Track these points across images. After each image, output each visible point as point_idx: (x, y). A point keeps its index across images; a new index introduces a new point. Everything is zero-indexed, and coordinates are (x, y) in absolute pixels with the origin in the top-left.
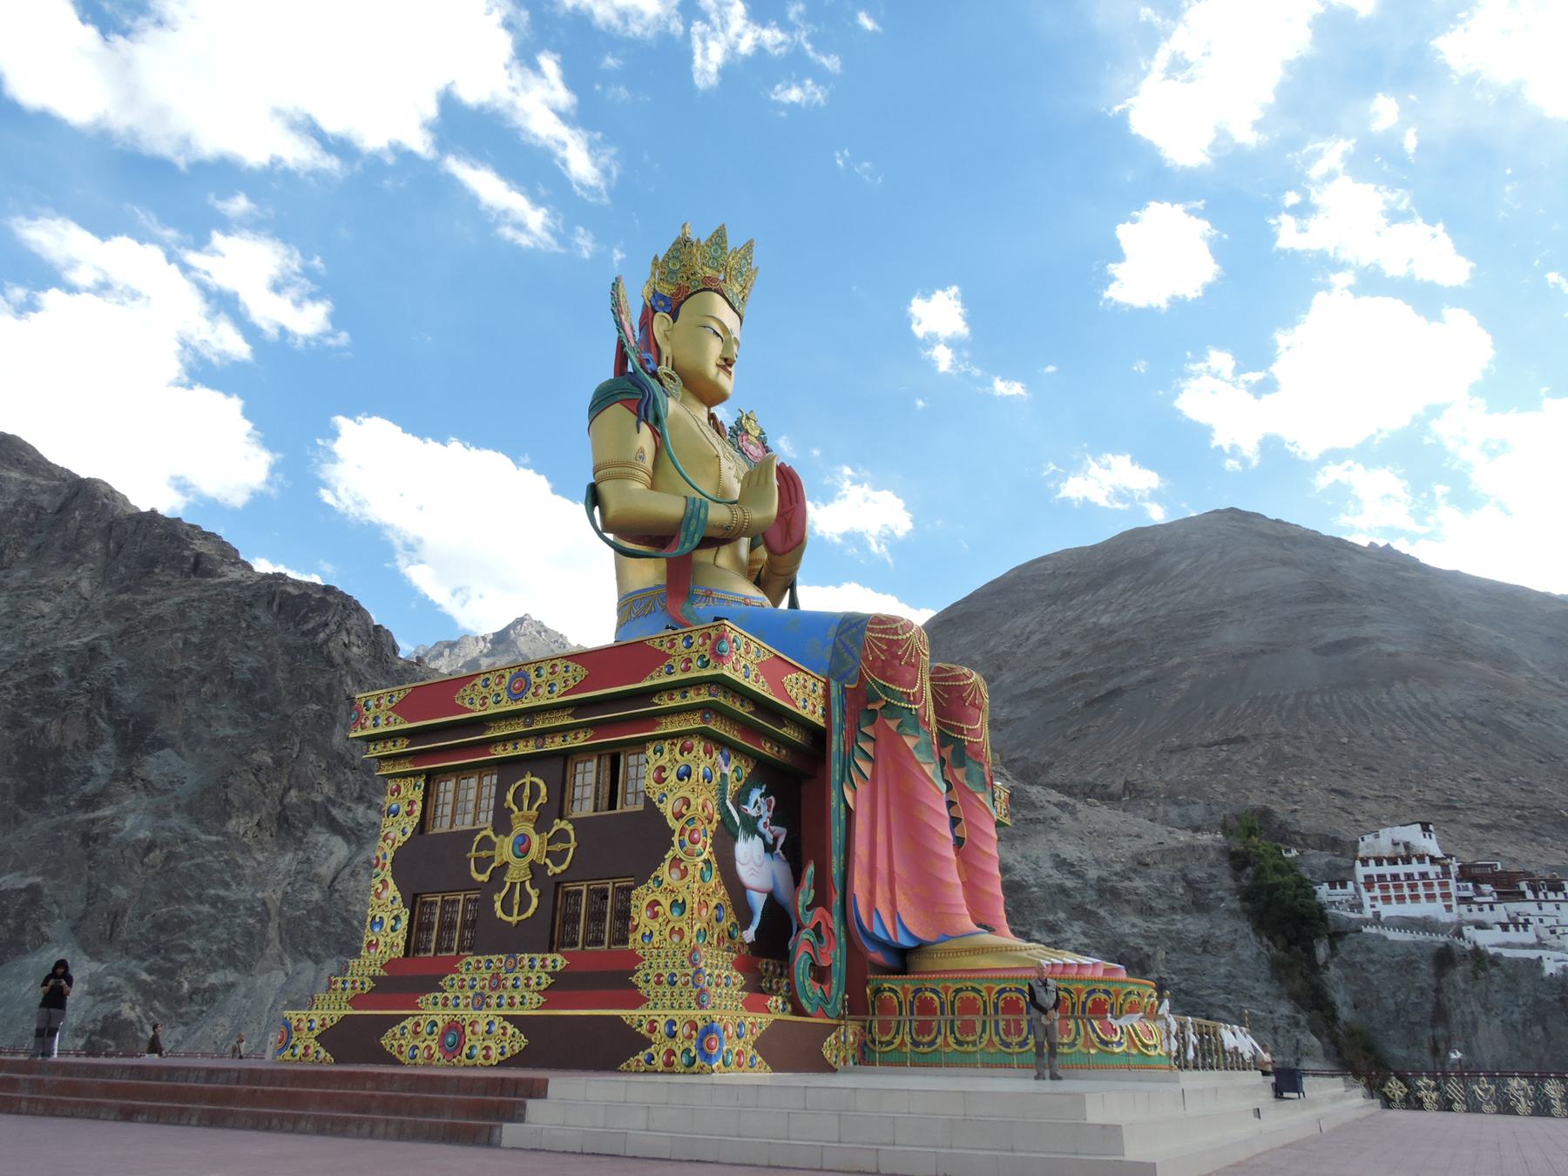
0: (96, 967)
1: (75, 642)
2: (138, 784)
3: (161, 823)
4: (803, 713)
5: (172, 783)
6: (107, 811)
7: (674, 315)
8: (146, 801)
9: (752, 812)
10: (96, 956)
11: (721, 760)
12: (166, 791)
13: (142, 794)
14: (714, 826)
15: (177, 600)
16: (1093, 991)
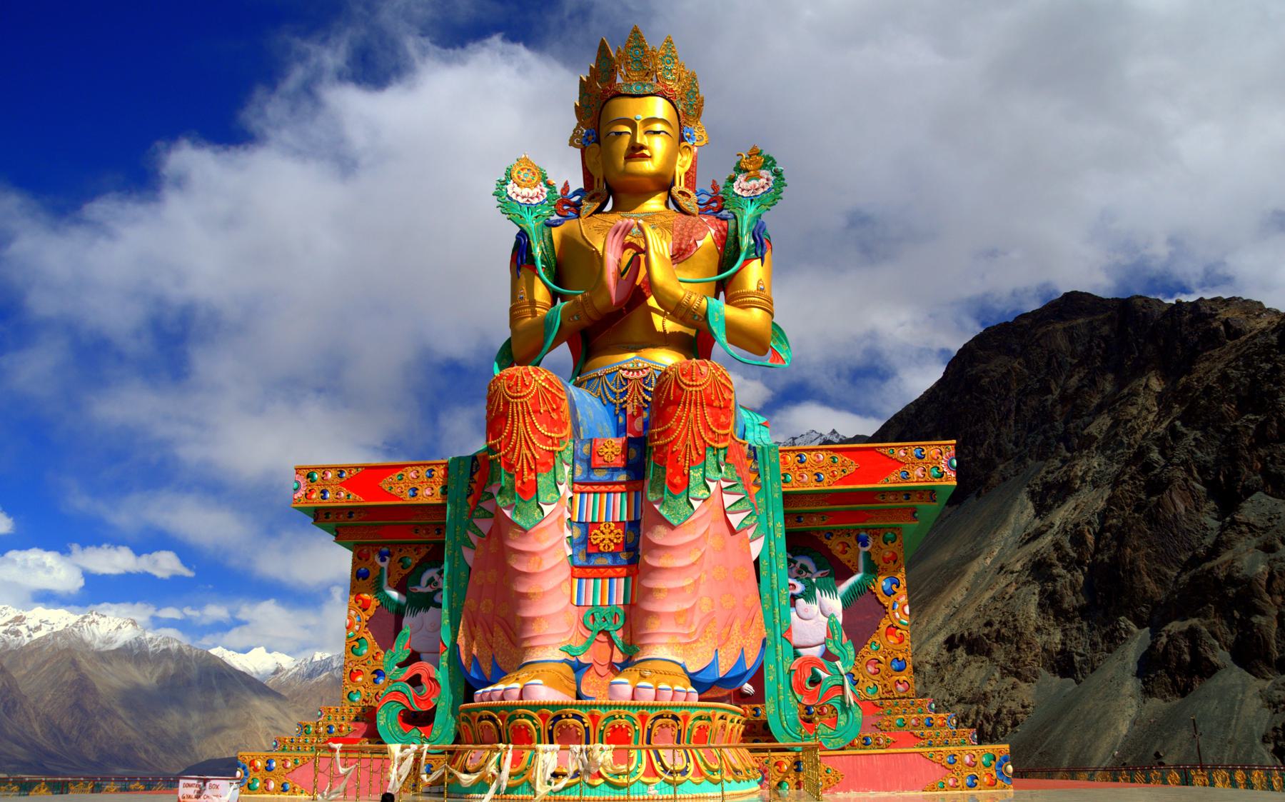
0: (1261, 683)
1: (1158, 430)
2: (1244, 528)
3: (1272, 556)
4: (414, 501)
5: (1270, 520)
6: (1226, 556)
7: (598, 141)
8: (1255, 541)
9: (423, 588)
10: (1258, 675)
11: (377, 559)
12: (1265, 530)
13: (1249, 535)
14: (371, 611)
15: (1220, 366)
16: (513, 718)
